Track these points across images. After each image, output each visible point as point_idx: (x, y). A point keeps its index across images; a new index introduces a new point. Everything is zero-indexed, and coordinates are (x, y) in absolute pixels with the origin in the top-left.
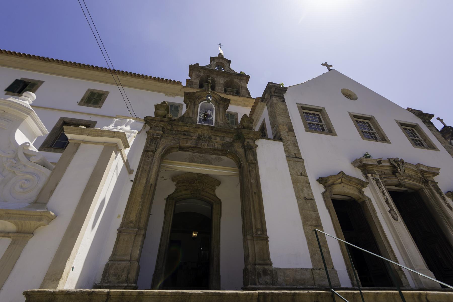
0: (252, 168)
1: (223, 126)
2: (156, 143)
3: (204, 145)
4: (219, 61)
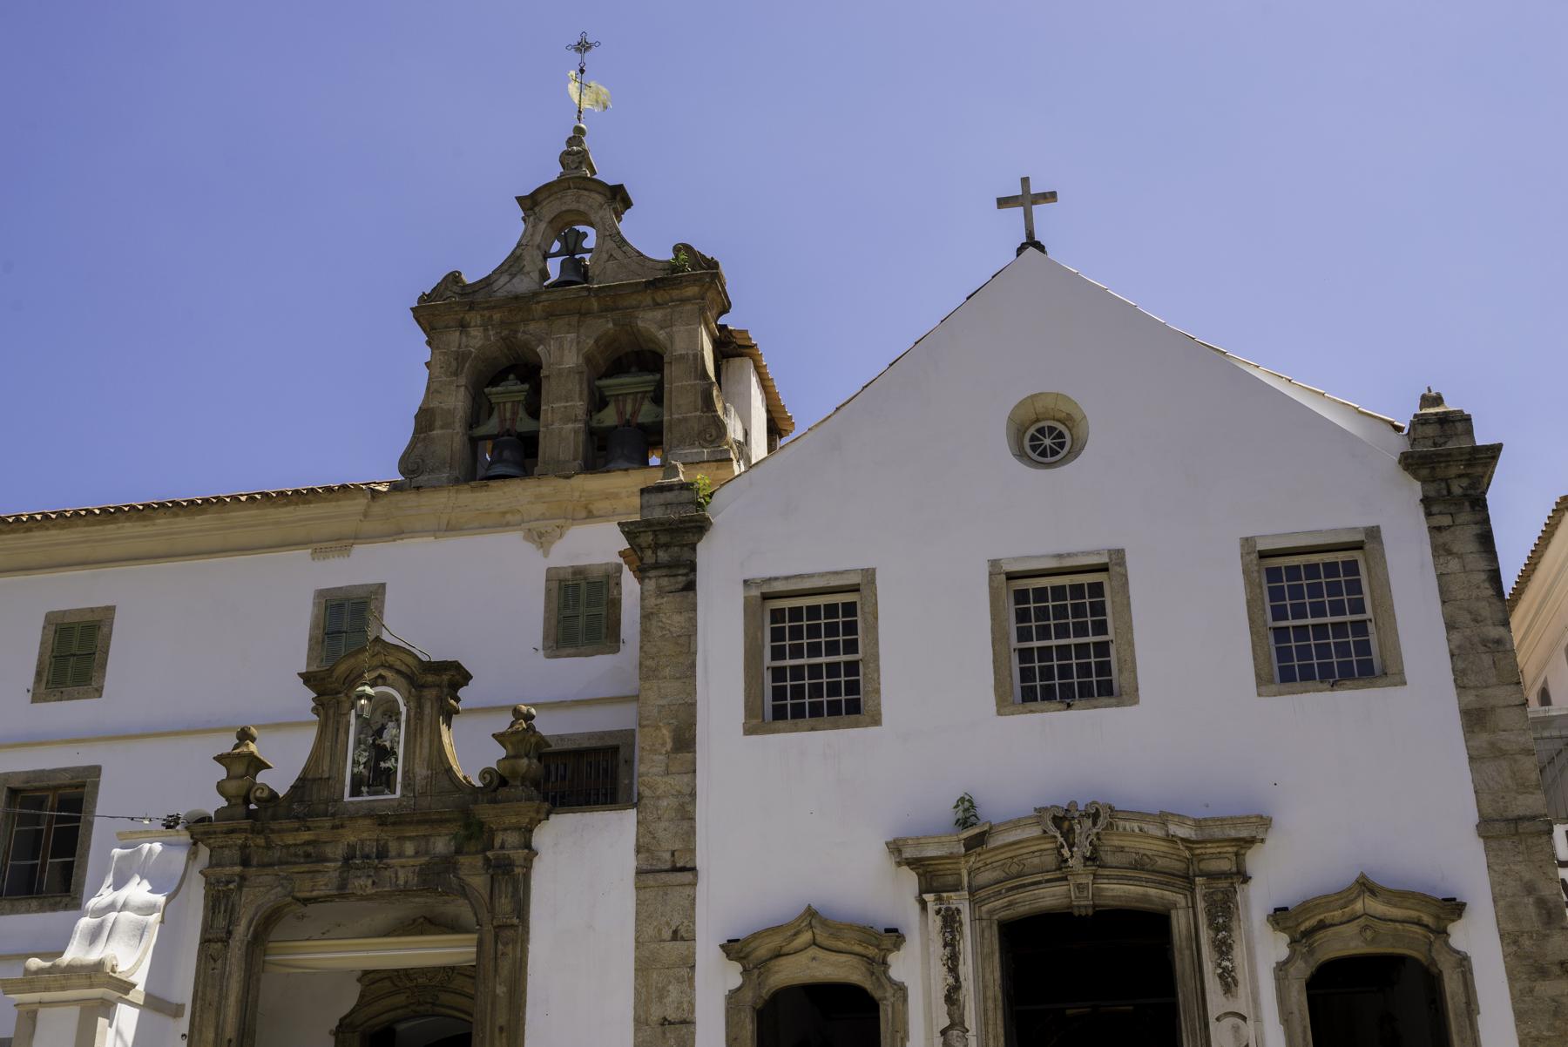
0: (506, 944)
1: (429, 787)
2: (229, 910)
3: (363, 886)
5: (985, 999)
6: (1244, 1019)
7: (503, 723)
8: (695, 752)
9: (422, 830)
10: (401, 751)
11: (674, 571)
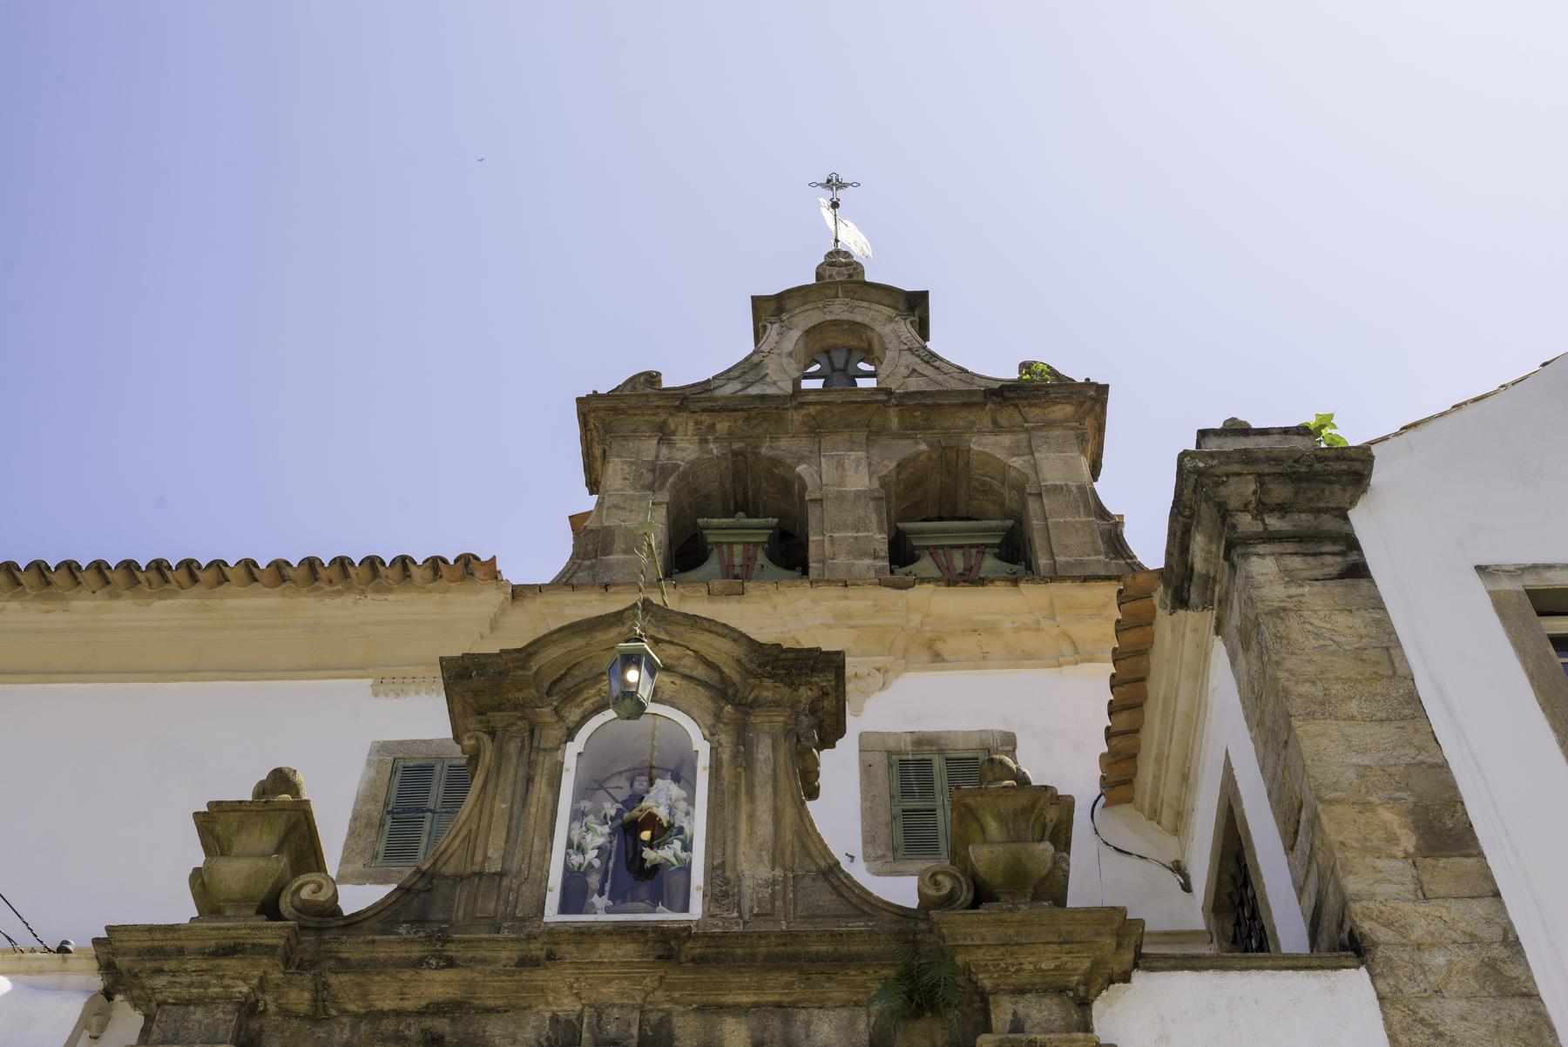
1: (779, 903)
4: (828, 318)
8: (1481, 855)
9: (776, 987)
11: (1313, 548)
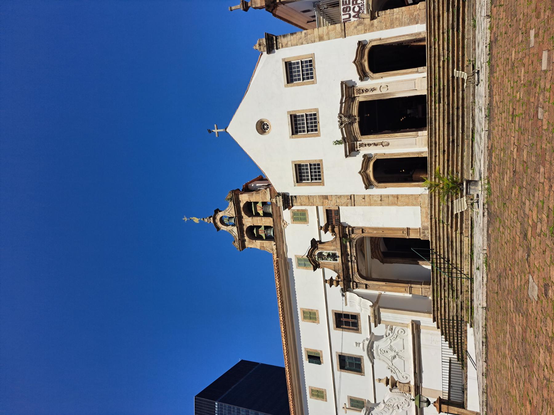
5: (377, 138)
6: (381, 86)
7: (322, 232)
10: (328, 252)
